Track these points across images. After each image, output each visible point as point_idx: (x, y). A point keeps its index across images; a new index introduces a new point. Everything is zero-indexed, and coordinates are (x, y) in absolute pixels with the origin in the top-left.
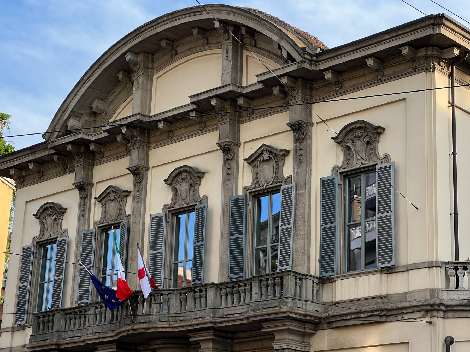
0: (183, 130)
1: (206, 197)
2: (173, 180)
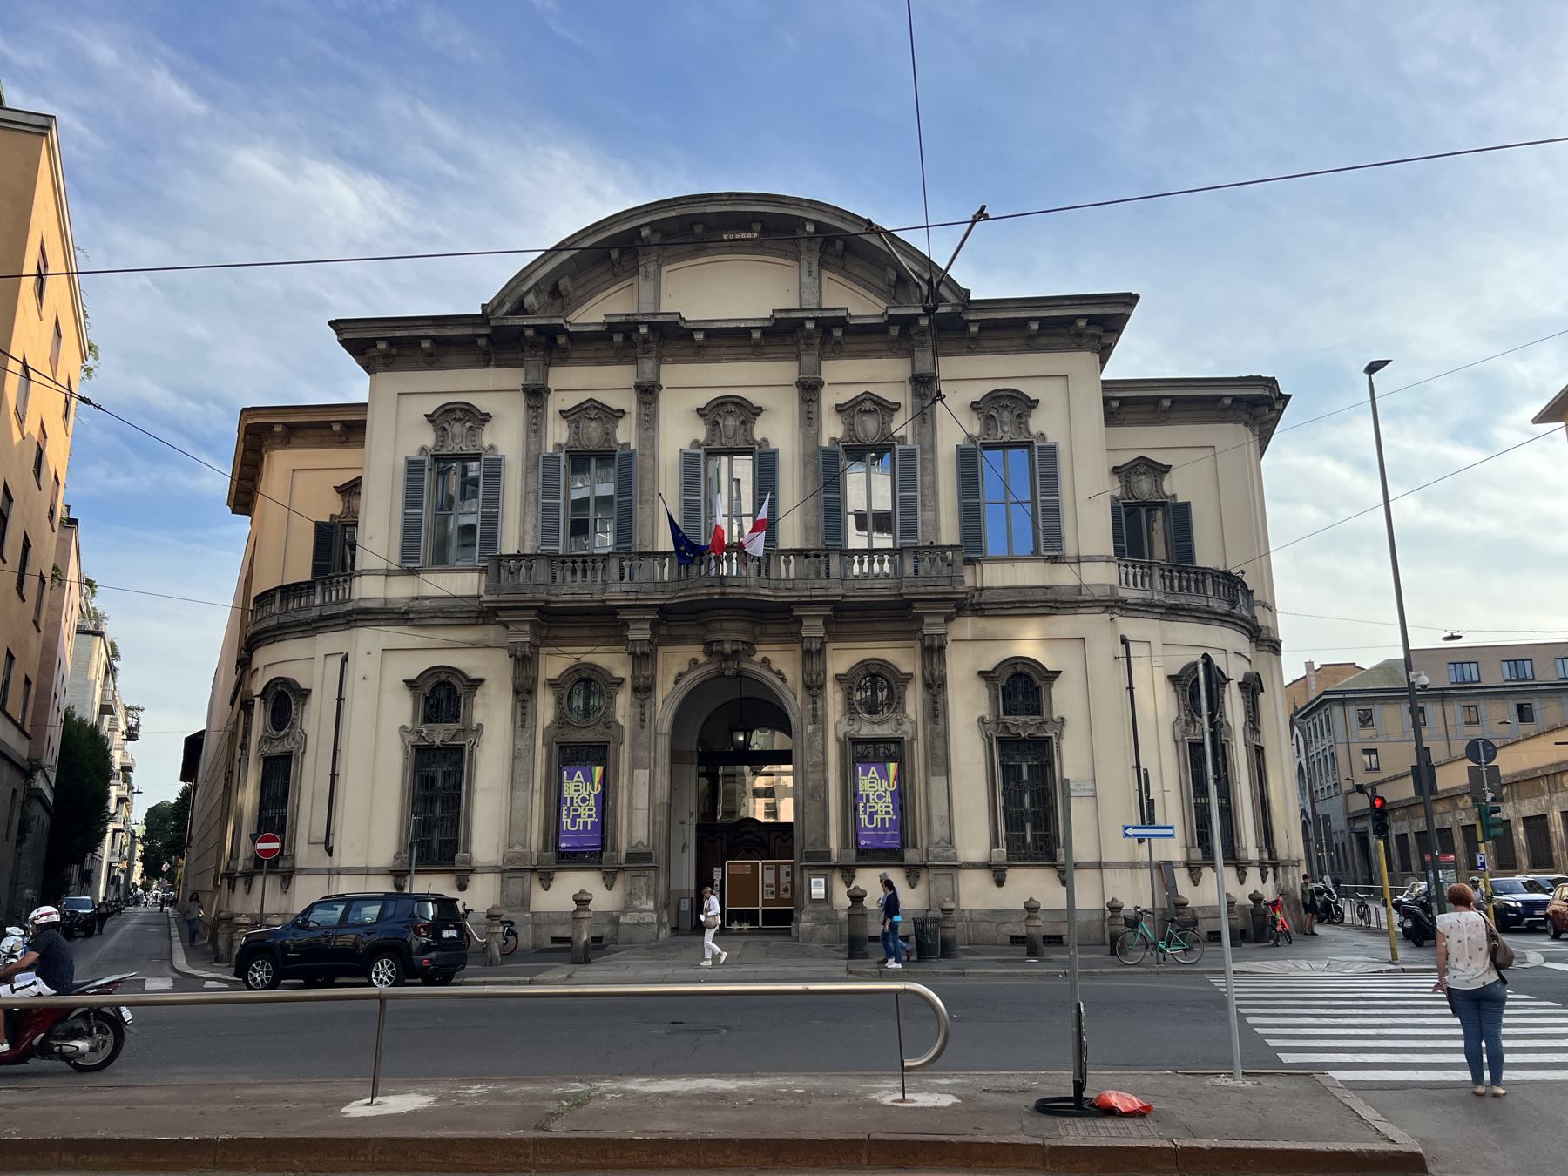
0: (724, 350)
1: (765, 441)
2: (712, 413)
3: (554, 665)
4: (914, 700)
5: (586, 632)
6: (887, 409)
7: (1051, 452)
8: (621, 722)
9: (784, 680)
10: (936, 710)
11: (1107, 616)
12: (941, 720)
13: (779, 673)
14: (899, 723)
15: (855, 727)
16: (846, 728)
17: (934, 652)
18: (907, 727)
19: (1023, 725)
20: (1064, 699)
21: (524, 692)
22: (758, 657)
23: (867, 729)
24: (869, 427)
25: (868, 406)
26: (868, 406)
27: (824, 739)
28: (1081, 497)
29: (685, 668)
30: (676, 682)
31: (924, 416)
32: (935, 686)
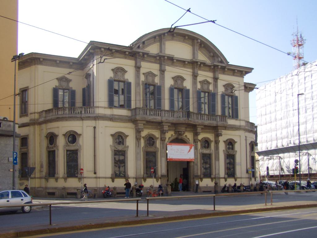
3: (144, 133)
4: (213, 145)
5: (150, 127)
6: (209, 83)
7: (237, 97)
8: (158, 147)
9: (189, 140)
10: (217, 148)
11: (244, 132)
12: (218, 150)
13: (189, 139)
14: (210, 150)
15: (203, 150)
16: (201, 151)
17: (217, 135)
18: (211, 151)
19: (231, 152)
20: (237, 147)
21: (138, 139)
22: (184, 135)
23: (206, 151)
24: (205, 87)
25: (205, 82)
26: (205, 82)
27: (198, 153)
28: (241, 108)
29: (170, 136)
30: (169, 139)
31: (216, 86)
32: (217, 142)
